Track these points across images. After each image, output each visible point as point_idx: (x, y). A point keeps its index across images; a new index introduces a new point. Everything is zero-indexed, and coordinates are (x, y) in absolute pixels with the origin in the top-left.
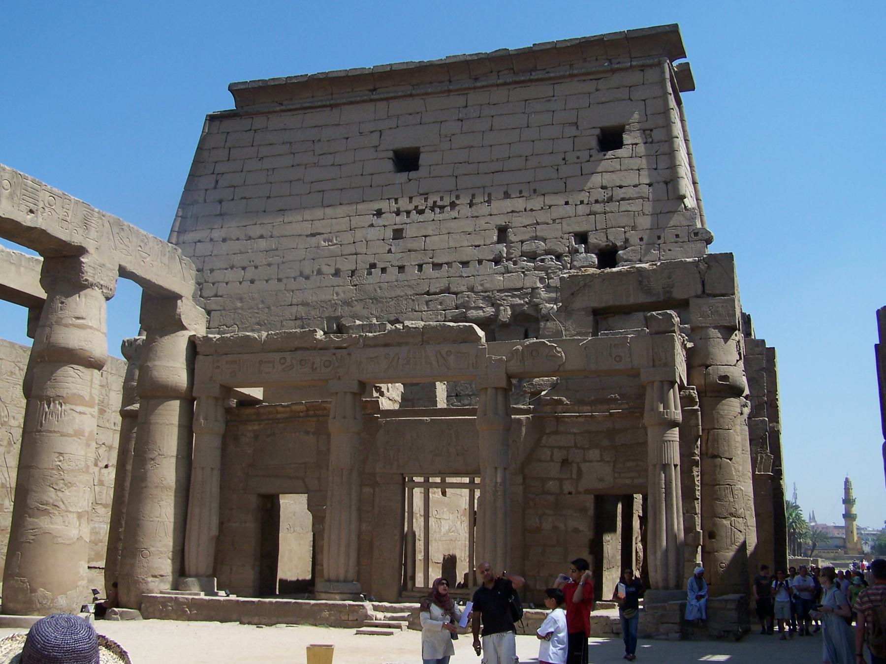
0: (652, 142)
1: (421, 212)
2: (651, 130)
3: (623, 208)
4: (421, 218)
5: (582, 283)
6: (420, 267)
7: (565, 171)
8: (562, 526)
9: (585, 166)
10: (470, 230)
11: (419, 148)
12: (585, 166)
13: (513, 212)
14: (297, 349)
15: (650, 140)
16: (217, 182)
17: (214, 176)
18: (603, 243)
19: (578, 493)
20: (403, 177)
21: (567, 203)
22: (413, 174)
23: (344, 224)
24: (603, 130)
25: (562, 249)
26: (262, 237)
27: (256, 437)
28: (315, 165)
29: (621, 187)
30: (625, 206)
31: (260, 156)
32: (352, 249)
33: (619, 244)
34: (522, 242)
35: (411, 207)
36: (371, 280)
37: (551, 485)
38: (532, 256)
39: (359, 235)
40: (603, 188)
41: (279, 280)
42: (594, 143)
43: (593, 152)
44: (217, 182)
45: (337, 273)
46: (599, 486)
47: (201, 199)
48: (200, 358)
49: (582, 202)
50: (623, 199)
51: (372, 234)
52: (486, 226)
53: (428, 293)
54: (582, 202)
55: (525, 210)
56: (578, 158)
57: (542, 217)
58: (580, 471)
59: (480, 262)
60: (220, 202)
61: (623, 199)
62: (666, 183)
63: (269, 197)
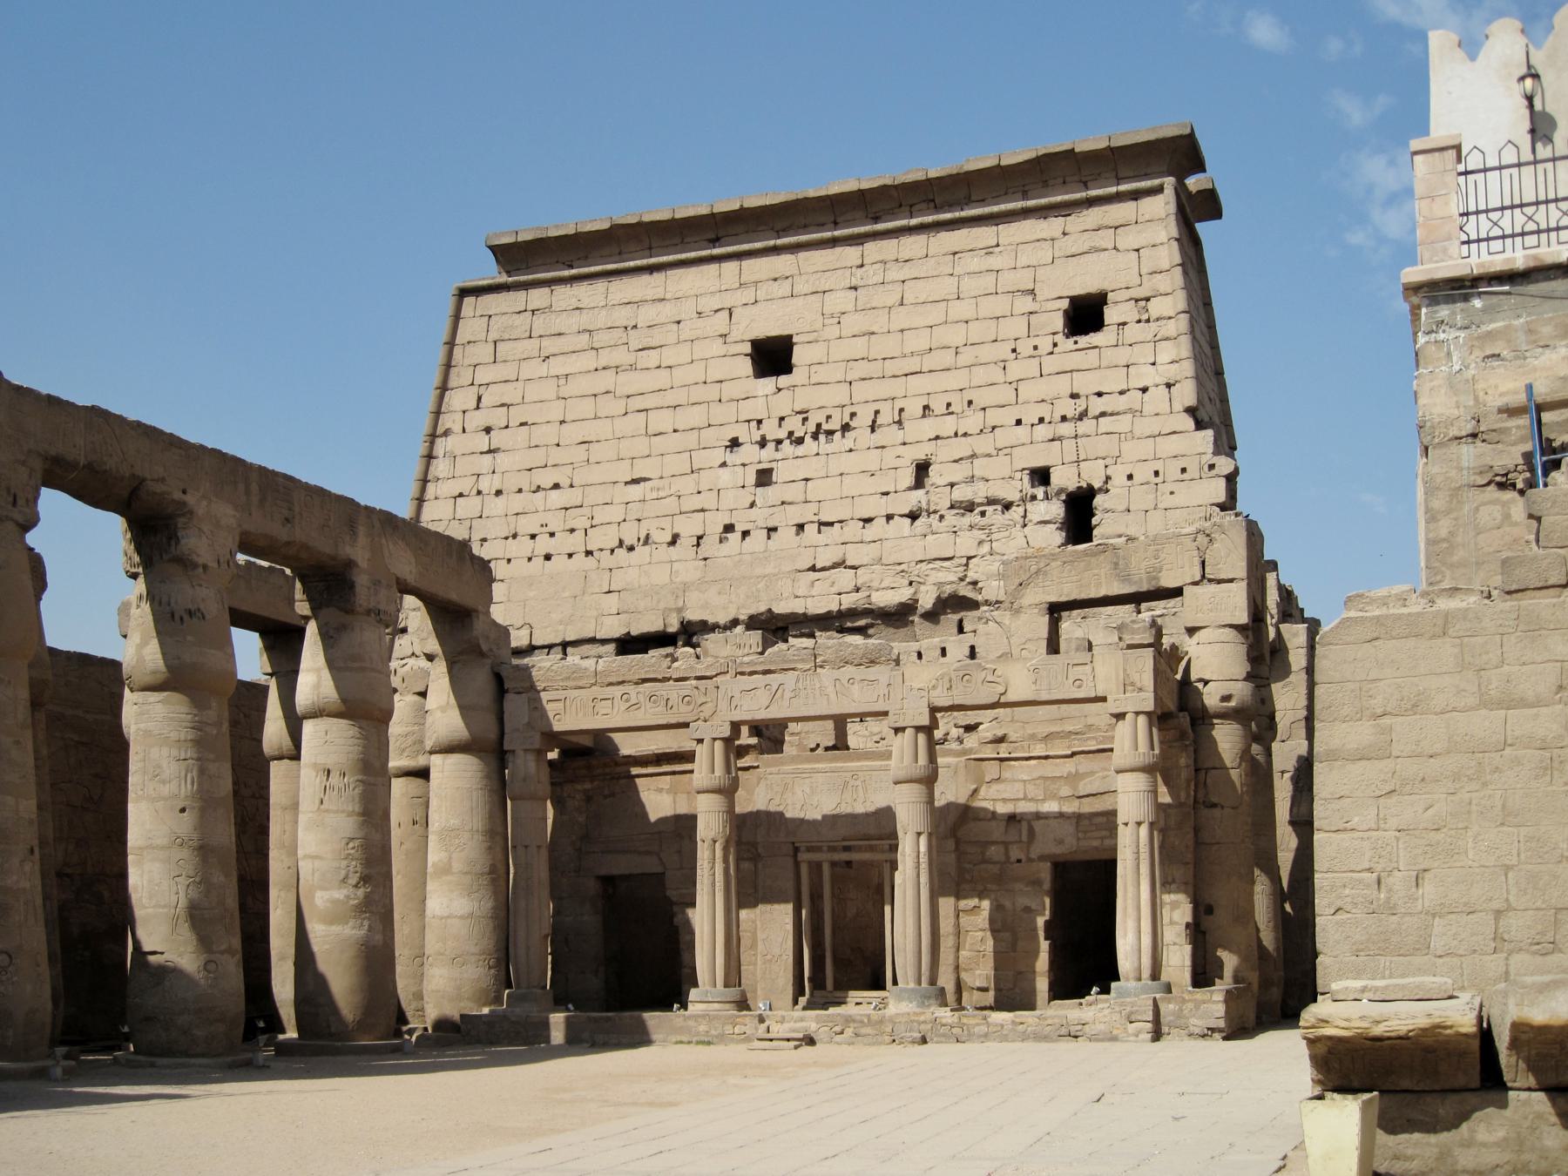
0: (1148, 321)
1: (800, 441)
2: (1148, 299)
3: (1102, 429)
4: (800, 450)
5: (1034, 569)
6: (801, 527)
7: (1016, 369)
8: (1008, 904)
9: (1047, 360)
10: (874, 467)
11: (790, 337)
12: (1047, 360)
13: (937, 438)
14: (645, 681)
15: (1145, 317)
16: (479, 398)
17: (475, 389)
19: (1030, 860)
20: (768, 384)
21: (1019, 422)
22: (783, 380)
23: (680, 464)
24: (1074, 300)
25: (1012, 495)
26: (556, 486)
27: (589, 799)
28: (633, 367)
29: (1100, 394)
31: (544, 354)
32: (697, 502)
34: (952, 485)
35: (782, 434)
36: (725, 549)
37: (994, 852)
38: (970, 507)
39: (706, 479)
40: (1074, 396)
41: (589, 553)
42: (1058, 322)
43: (1060, 338)
44: (479, 398)
45: (674, 540)
46: (1057, 850)
47: (457, 428)
48: (509, 697)
49: (1041, 420)
50: (1103, 414)
51: (725, 476)
52: (898, 462)
53: (813, 569)
55: (956, 434)
56: (1035, 348)
57: (983, 444)
58: (1032, 833)
59: (889, 517)
60: (488, 430)
61: (1103, 414)
62: (1169, 386)
63: (562, 422)
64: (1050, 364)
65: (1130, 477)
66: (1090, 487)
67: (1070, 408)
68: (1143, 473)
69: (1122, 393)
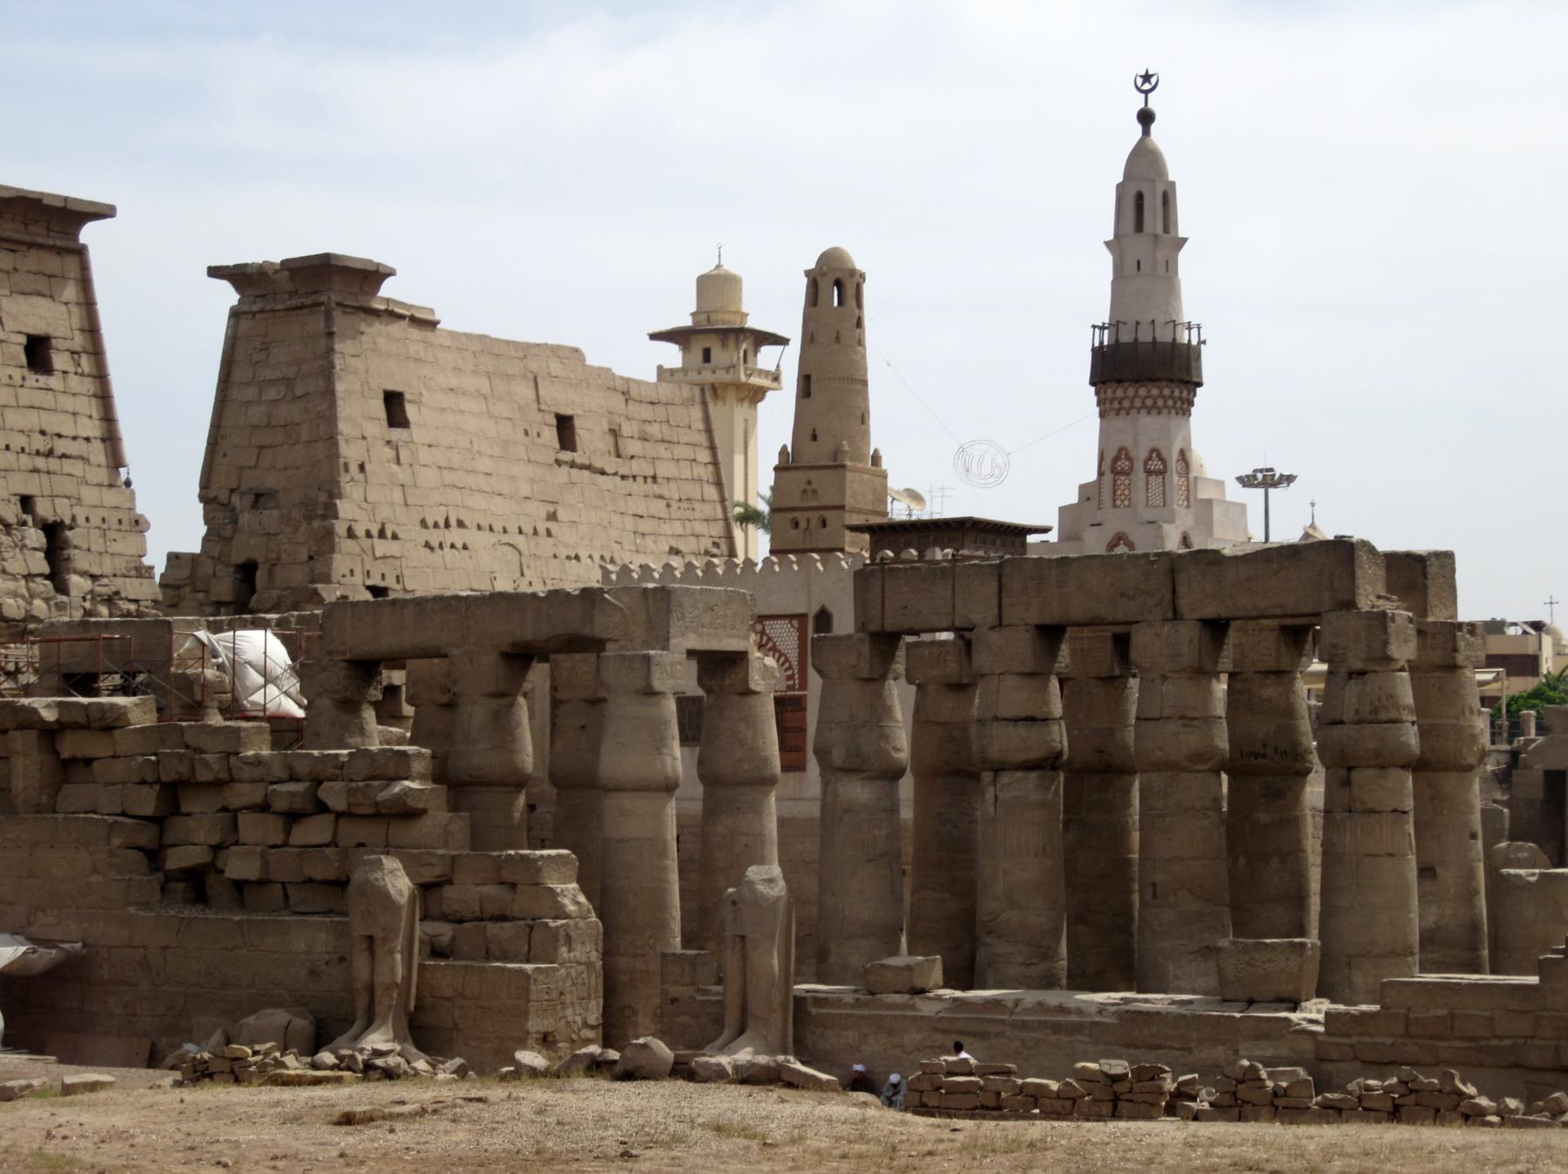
18: (51, 519)
30: (68, 466)
33: (68, 521)
40: (43, 433)
50: (63, 456)
54: (23, 450)
61: (63, 456)
64: (25, 396)
65: (87, 519)
66: (62, 522)
67: (40, 443)
68: (95, 521)
69: (74, 438)
